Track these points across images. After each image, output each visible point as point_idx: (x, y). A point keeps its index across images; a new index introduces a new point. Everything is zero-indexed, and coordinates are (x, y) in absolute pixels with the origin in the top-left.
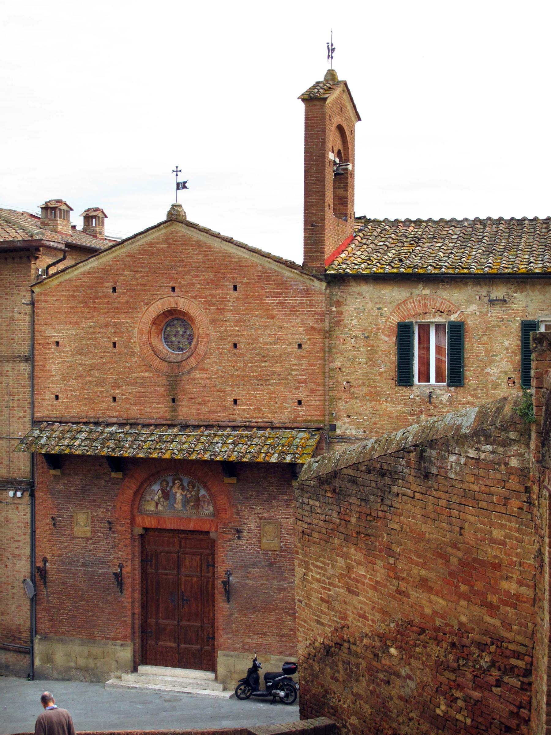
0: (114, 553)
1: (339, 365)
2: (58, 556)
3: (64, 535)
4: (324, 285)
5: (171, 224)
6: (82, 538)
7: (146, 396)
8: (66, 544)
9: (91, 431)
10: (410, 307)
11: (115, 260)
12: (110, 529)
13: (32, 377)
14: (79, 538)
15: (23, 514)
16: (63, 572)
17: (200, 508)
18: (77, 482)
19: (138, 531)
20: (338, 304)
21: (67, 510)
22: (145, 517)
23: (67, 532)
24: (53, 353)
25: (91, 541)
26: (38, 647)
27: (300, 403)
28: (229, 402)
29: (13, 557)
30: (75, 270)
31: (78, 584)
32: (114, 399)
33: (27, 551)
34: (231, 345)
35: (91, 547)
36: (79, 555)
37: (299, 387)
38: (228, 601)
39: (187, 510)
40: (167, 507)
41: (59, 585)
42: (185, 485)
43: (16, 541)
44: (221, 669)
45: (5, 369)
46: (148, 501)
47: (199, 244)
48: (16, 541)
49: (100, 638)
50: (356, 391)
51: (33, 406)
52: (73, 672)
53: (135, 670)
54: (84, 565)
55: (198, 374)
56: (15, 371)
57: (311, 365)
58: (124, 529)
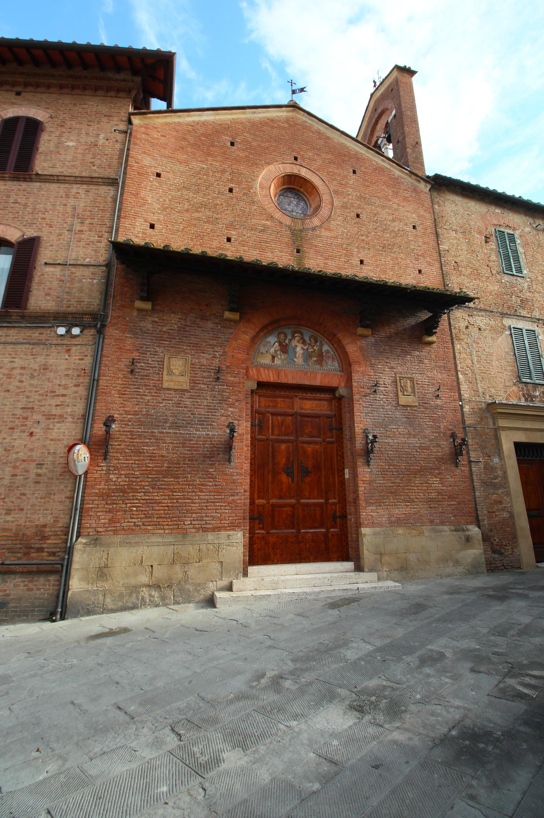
1: (447, 248)
2: (133, 415)
3: (145, 385)
4: (429, 186)
6: (175, 390)
7: (266, 242)
8: (148, 398)
11: (234, 121)
12: (218, 378)
14: (169, 389)
15: (77, 358)
16: (140, 436)
17: (324, 363)
18: (173, 322)
21: (155, 353)
22: (262, 369)
23: (151, 382)
24: (151, 182)
26: (81, 558)
27: (420, 271)
29: (50, 419)
30: (188, 116)
31: (164, 453)
32: (229, 240)
33: (79, 408)
34: (353, 214)
35: (188, 402)
36: (168, 413)
38: (368, 463)
40: (289, 358)
41: (131, 456)
42: (307, 339)
43: (58, 396)
44: (367, 554)
45: (74, 191)
46: (262, 353)
47: (319, 133)
48: (58, 396)
49: (193, 530)
52: (145, 592)
53: (245, 574)
54: (175, 426)
55: (324, 233)
56: (90, 194)
57: (425, 243)
58: (237, 380)
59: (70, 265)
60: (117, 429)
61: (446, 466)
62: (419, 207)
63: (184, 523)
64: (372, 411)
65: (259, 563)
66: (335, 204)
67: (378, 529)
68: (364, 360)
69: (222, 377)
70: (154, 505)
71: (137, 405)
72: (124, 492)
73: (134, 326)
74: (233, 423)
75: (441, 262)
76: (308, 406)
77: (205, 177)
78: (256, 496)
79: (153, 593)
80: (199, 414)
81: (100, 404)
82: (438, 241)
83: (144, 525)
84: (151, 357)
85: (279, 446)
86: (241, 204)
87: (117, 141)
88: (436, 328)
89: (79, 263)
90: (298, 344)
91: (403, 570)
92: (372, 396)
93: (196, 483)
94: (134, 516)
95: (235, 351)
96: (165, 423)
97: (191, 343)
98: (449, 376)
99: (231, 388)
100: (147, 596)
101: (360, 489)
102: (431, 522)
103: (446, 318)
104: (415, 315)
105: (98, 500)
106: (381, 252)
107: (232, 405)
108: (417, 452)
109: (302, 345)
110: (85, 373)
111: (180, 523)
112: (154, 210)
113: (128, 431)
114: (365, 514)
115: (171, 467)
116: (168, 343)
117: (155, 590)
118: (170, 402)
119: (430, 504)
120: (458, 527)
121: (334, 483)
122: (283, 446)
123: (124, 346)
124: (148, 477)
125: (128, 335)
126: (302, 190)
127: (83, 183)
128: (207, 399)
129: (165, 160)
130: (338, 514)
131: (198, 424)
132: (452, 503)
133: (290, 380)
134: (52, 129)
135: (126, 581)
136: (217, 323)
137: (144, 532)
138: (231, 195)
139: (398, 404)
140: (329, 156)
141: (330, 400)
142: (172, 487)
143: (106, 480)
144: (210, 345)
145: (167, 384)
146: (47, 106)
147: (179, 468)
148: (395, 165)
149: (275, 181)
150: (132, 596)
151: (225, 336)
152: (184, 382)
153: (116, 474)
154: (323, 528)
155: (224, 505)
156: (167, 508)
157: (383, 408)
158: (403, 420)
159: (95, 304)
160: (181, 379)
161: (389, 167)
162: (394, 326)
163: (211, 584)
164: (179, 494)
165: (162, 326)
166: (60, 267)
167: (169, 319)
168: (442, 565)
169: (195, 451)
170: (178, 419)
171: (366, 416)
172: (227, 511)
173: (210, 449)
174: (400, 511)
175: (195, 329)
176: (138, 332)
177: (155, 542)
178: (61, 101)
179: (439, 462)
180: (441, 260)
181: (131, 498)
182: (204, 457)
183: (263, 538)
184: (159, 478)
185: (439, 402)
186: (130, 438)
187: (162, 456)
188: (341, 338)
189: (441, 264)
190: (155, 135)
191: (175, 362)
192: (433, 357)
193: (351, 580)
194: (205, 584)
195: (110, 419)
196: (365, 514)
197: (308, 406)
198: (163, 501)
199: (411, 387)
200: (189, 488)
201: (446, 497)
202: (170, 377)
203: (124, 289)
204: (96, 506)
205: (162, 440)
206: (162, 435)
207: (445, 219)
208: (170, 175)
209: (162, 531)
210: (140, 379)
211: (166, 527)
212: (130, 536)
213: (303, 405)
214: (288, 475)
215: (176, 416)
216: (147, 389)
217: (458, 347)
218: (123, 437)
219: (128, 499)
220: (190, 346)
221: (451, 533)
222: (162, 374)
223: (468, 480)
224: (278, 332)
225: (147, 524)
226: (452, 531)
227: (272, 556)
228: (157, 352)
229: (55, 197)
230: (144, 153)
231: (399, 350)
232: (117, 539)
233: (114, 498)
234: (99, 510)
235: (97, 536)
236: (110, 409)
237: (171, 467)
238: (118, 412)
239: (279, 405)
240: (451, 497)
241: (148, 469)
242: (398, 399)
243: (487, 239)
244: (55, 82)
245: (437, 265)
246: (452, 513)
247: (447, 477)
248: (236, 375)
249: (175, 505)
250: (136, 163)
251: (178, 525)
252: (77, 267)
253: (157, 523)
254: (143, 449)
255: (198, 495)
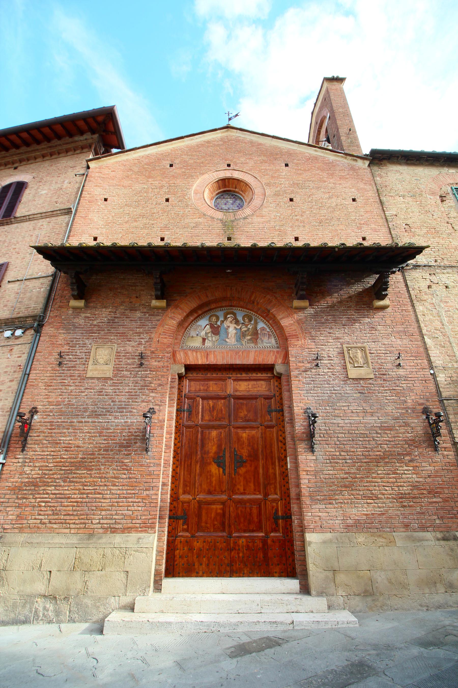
0: (144, 395)
1: (395, 213)
2: (56, 405)
3: (71, 376)
4: (367, 163)
5: (227, 131)
6: (98, 379)
8: (72, 388)
12: (141, 364)
14: (92, 378)
15: (16, 356)
22: (189, 353)
23: (77, 372)
24: (99, 205)
25: (110, 382)
31: (80, 443)
35: (110, 390)
36: (90, 402)
37: (361, 227)
38: (312, 449)
39: (242, 345)
42: (240, 318)
46: (192, 337)
49: (101, 531)
50: (417, 230)
52: (40, 604)
53: (158, 587)
58: (161, 364)
59: (25, 280)
60: (38, 420)
61: (421, 450)
62: (358, 182)
63: (92, 522)
64: (314, 387)
65: (181, 575)
66: (267, 194)
67: (329, 536)
68: (303, 333)
69: (146, 363)
70: (63, 500)
71: (60, 395)
72: (36, 485)
73: (68, 323)
74: (153, 408)
75: (389, 227)
76: (244, 387)
77: (145, 194)
78: (181, 491)
79: (48, 606)
80: (119, 402)
81: (27, 397)
82: (383, 208)
83: (50, 523)
84: (79, 349)
85: (209, 433)
86: (176, 209)
87: (77, 182)
88: (386, 289)
89: (33, 277)
90: (230, 325)
91: (369, 595)
92: (313, 370)
93: (108, 475)
94: (42, 513)
95: (161, 336)
96: (84, 412)
97: (119, 333)
98: (411, 341)
99: (154, 373)
100: (41, 609)
101: (302, 481)
102: (407, 526)
103: (402, 280)
104: (361, 282)
105: (10, 494)
106: (318, 227)
107: (153, 390)
108: (377, 433)
109: (235, 325)
110: (20, 368)
111: (87, 521)
112: (98, 226)
113: (48, 422)
114: (310, 514)
115: (85, 458)
116: (96, 335)
117: (51, 603)
118: (92, 391)
119: (402, 502)
120: (447, 535)
121: (275, 474)
122: (214, 433)
123: (57, 341)
124: (61, 470)
125: (61, 332)
126: (237, 190)
127: (46, 217)
128: (129, 386)
129: (112, 188)
130: (280, 514)
131: (117, 412)
132: (434, 500)
133: (220, 360)
134: (33, 186)
135: (21, 588)
136: (145, 313)
137: (49, 531)
138: (167, 203)
139: (348, 377)
140: (263, 158)
141: (267, 380)
142: (83, 480)
143: (21, 473)
144: (136, 333)
145: (91, 373)
146: (33, 171)
147: (93, 459)
148: (329, 152)
149: (209, 186)
150: (25, 607)
151: (152, 323)
152: (108, 371)
153: (31, 466)
154: (262, 532)
155: (137, 500)
156: (75, 504)
157: (328, 384)
158: (355, 395)
159: (39, 308)
160: (105, 367)
161: (322, 155)
162: (336, 294)
163: (112, 600)
164: (90, 488)
165: (93, 320)
166: (18, 283)
167: (101, 313)
168: (427, 591)
169: (111, 440)
170: (98, 408)
171: (307, 393)
172: (140, 508)
173: (127, 438)
174: (360, 510)
175: (123, 320)
176: (71, 328)
177: (56, 543)
178: (42, 166)
179: (409, 445)
180: (388, 225)
181: (41, 492)
182: (120, 447)
183: (187, 542)
184: (72, 470)
185: (401, 372)
186: (49, 429)
187: (78, 447)
188: (274, 313)
189: (390, 229)
190: (106, 171)
191: (101, 352)
192: (389, 322)
193: (289, 607)
194: (107, 598)
195: (34, 410)
196: (310, 514)
197: (244, 387)
198: (73, 496)
199: (362, 357)
200: (101, 482)
201: (425, 492)
202: (95, 367)
203: (64, 292)
204: (7, 500)
205: (79, 429)
206: (81, 424)
207: (389, 188)
208: (115, 198)
209: (67, 531)
210: (67, 370)
211: (72, 526)
212: (34, 535)
213: (238, 387)
214: (219, 465)
215: (97, 405)
216: (72, 379)
217: (420, 308)
218: (42, 428)
219: (39, 494)
220: (117, 336)
221: (437, 542)
222: (88, 364)
223: (455, 468)
224: (209, 315)
225: (54, 521)
226: (438, 540)
227: (196, 567)
228: (85, 344)
229: (26, 231)
230: (96, 186)
231: (344, 320)
232: (21, 538)
233: (25, 492)
234: (9, 504)
235: (3, 534)
236: (35, 401)
237: (85, 458)
238: (42, 403)
239: (211, 389)
240: (432, 492)
241: (62, 460)
242: (347, 372)
243: (443, 198)
244: (39, 153)
245: (385, 230)
246: (435, 514)
247: (423, 464)
248: (160, 359)
249: (84, 500)
250: (89, 194)
251: (85, 524)
252: (31, 280)
253: (64, 521)
254: (60, 440)
255: (110, 490)
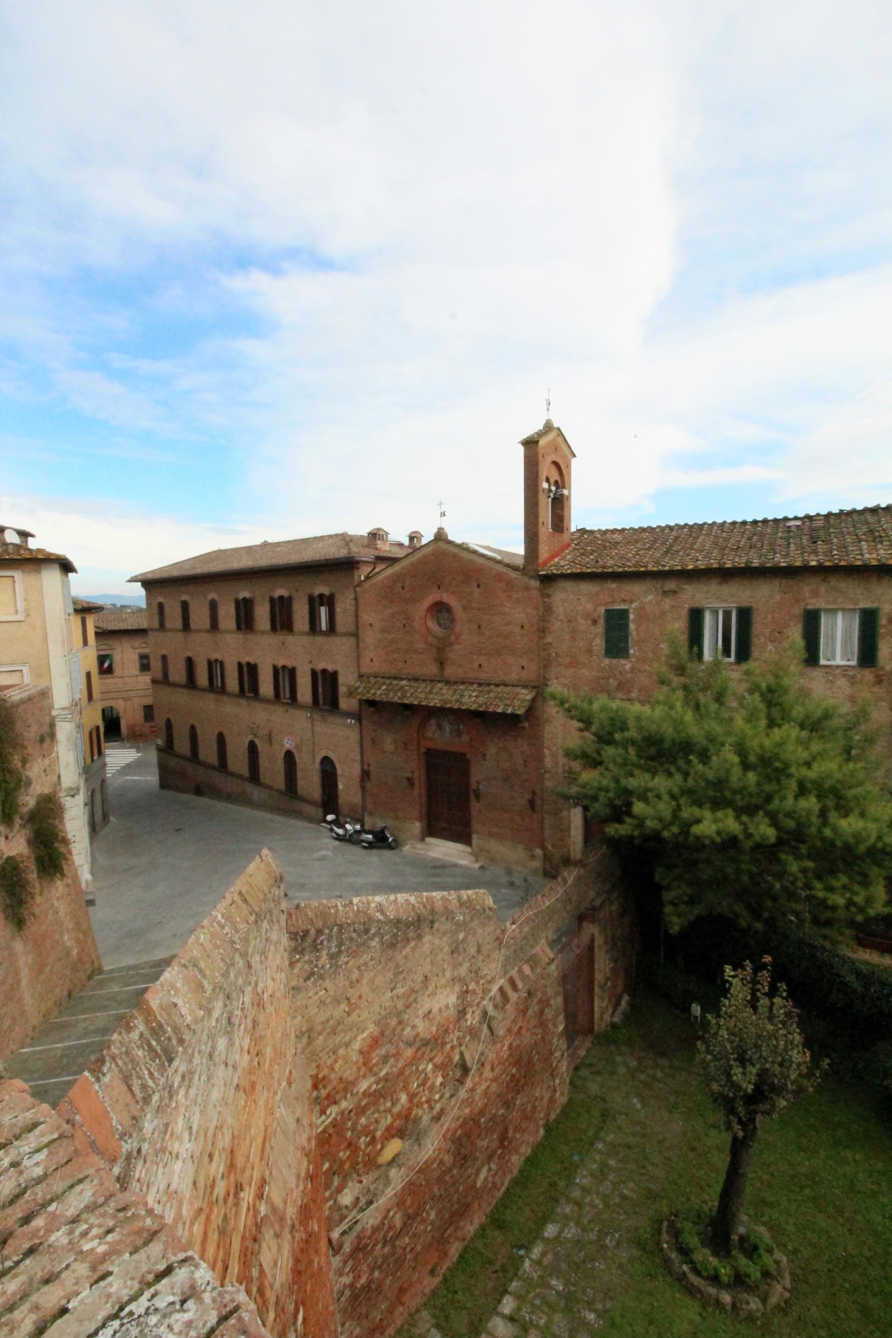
4: (538, 583)
9: (391, 684)
10: (601, 597)
13: (358, 646)
19: (423, 750)
20: (549, 596)
27: (523, 667)
28: (476, 665)
33: (358, 758)
34: (476, 626)
47: (455, 556)
51: (359, 666)
102: (513, 841)
